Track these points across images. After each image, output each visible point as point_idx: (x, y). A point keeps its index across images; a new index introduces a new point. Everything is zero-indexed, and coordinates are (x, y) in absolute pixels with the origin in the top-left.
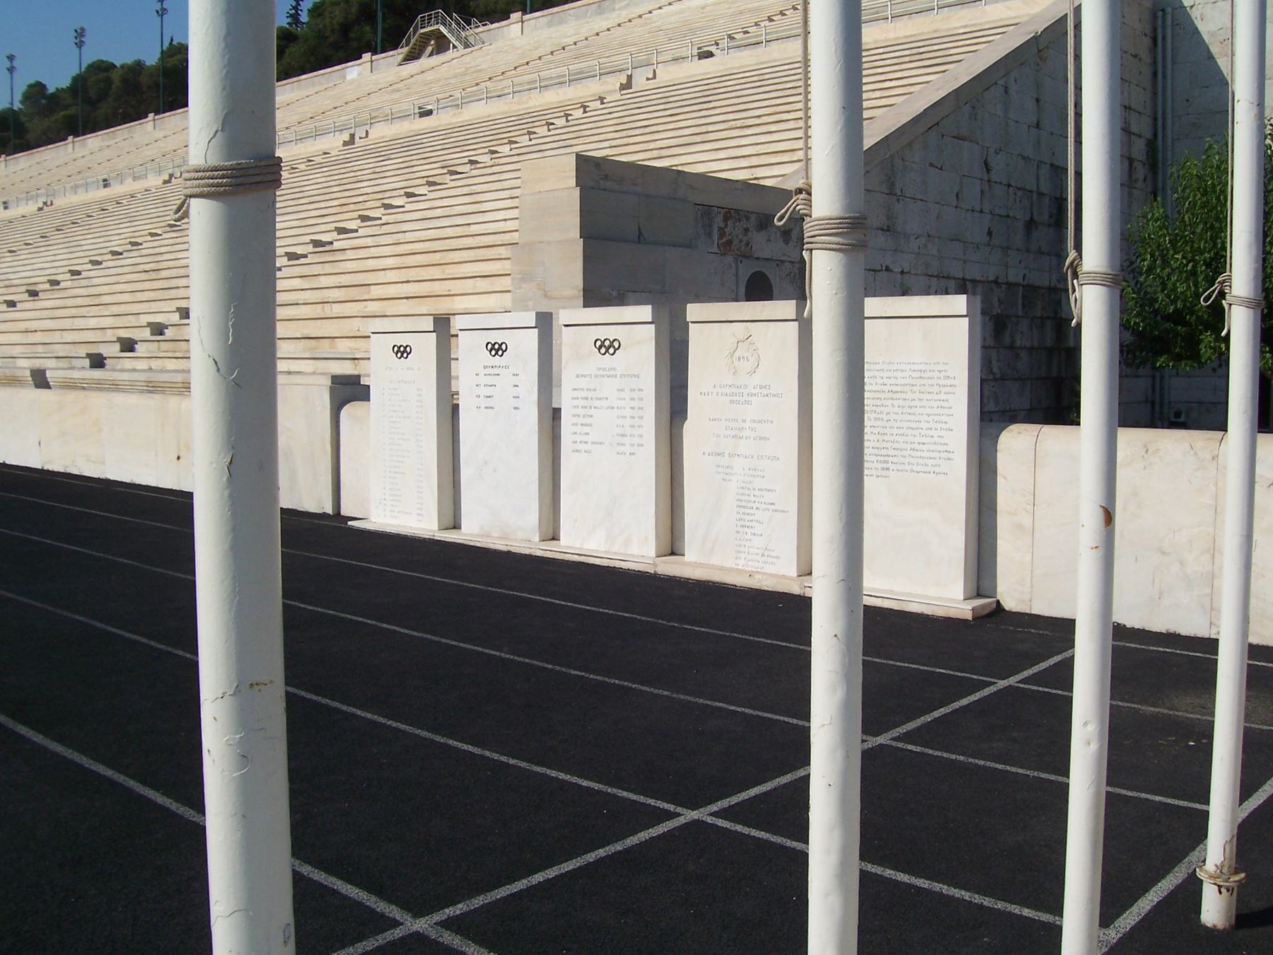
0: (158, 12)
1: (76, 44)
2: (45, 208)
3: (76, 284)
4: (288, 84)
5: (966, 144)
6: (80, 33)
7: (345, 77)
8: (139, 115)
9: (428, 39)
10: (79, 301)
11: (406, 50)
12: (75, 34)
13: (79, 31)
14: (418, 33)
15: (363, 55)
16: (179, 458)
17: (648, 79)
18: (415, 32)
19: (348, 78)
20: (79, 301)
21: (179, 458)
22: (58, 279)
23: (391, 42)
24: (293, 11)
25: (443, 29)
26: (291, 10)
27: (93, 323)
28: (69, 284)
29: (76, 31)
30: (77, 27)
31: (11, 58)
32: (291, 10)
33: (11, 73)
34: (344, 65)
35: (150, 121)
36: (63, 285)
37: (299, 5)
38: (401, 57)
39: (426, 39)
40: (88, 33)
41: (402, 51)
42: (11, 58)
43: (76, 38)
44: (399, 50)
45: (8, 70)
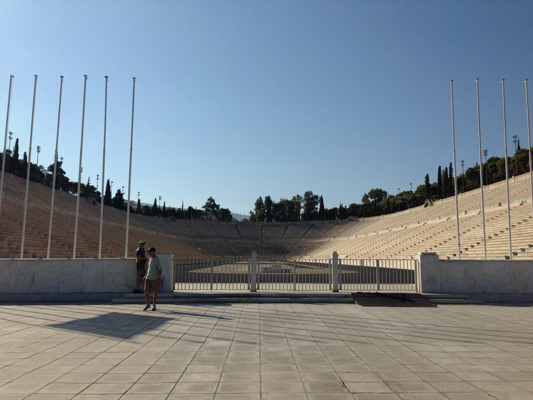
0: (514, 142)
1: (484, 155)
2: (480, 213)
3: (497, 238)
6: (486, 151)
10: (499, 243)
20: (499, 243)
22: (491, 236)
27: (504, 248)
28: (494, 238)
29: (484, 151)
30: (485, 150)
31: (462, 162)
36: (493, 238)
42: (462, 162)
43: (484, 153)
45: (462, 165)
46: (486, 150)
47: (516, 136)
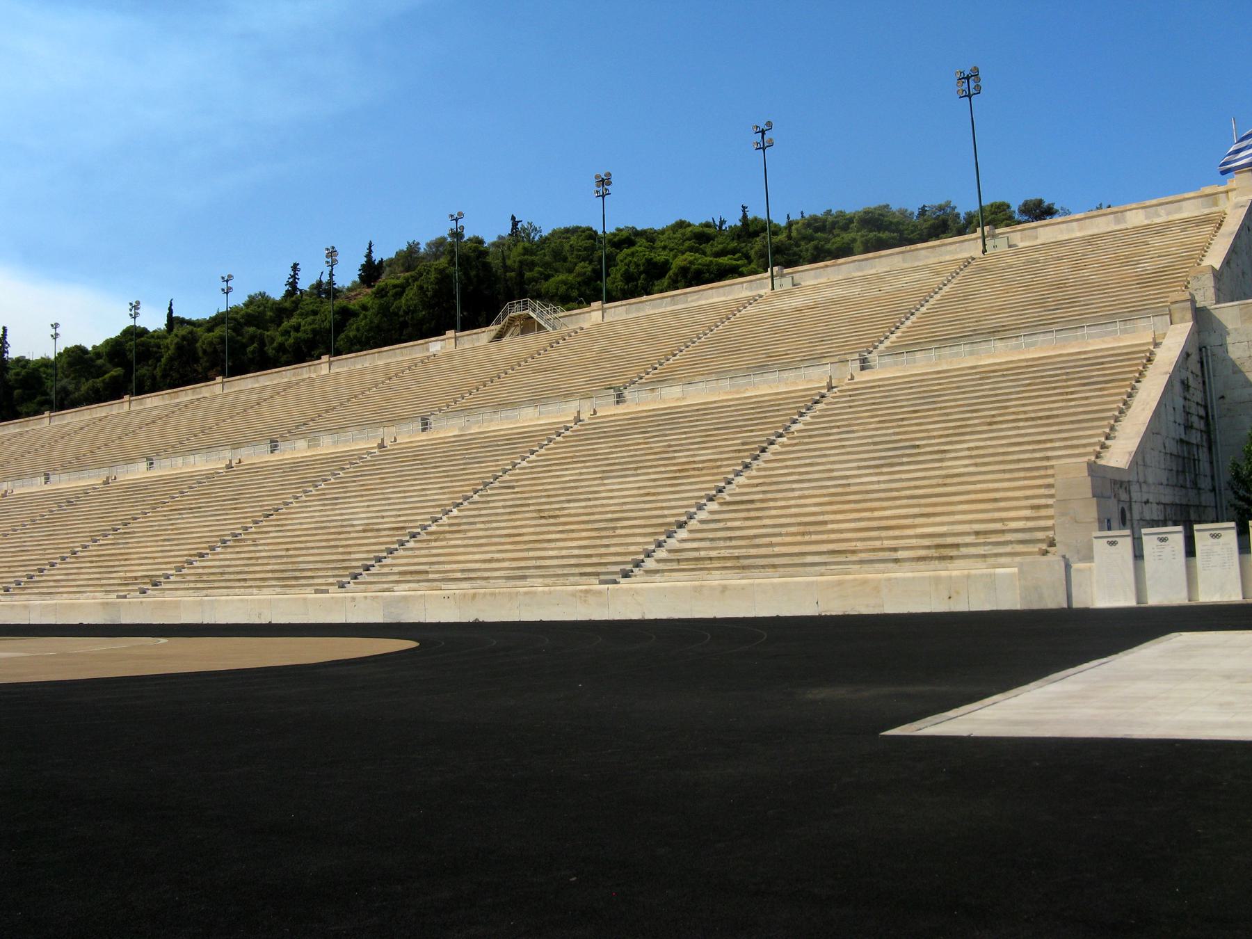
1: (131, 315)
4: (369, 354)
5: (1159, 436)
7: (428, 350)
8: (206, 378)
9: (513, 321)
11: (498, 327)
12: (130, 307)
13: (134, 304)
14: (508, 316)
15: (447, 332)
16: (950, 598)
17: (849, 380)
18: (505, 315)
19: (431, 351)
21: (950, 598)
23: (471, 323)
24: (291, 280)
25: (532, 314)
26: (289, 278)
29: (131, 304)
32: (289, 278)
33: (55, 339)
34: (427, 340)
35: (218, 383)
37: (297, 274)
38: (493, 334)
39: (512, 320)
40: (141, 306)
41: (494, 328)
42: (55, 326)
43: (131, 310)
44: (491, 328)
46: (138, 303)
47: (230, 277)
